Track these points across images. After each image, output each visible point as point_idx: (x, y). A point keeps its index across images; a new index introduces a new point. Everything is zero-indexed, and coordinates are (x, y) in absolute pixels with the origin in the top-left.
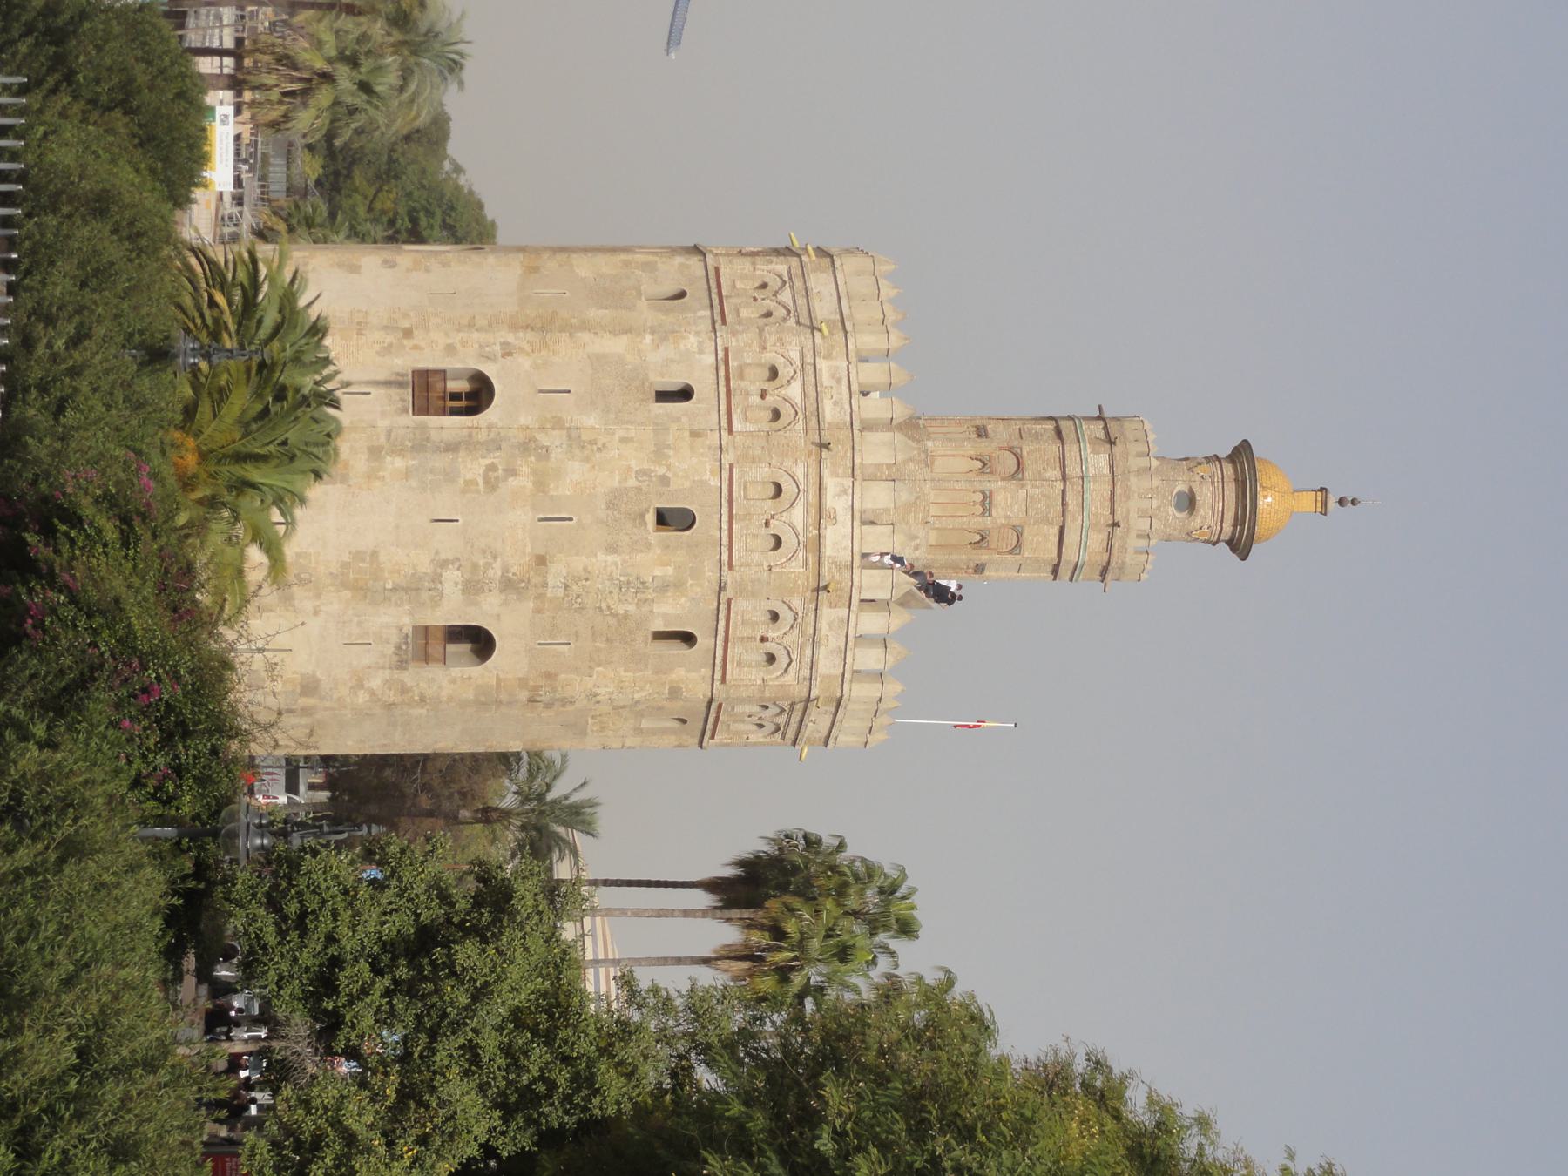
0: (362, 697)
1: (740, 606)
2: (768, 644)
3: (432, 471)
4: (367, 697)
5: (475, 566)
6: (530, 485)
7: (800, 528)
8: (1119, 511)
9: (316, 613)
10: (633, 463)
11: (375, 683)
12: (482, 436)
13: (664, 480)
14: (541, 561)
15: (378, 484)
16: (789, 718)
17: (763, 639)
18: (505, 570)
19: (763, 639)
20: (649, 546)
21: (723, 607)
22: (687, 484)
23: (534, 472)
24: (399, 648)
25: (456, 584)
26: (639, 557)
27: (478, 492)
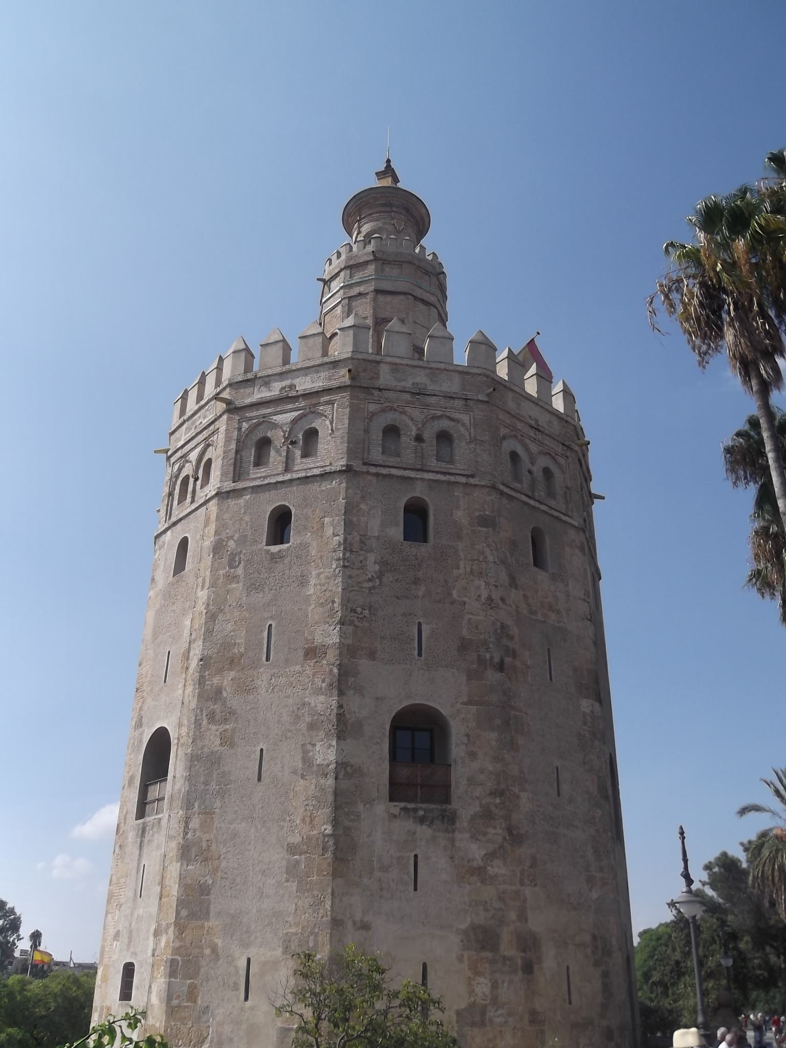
0: (497, 868)
1: (376, 454)
2: (426, 435)
3: (206, 783)
4: (497, 862)
5: (312, 727)
6: (232, 674)
7: (296, 414)
8: (367, 259)
9: (365, 927)
10: (221, 572)
11: (476, 851)
12: (184, 731)
13: (242, 541)
14: (312, 652)
15: (214, 847)
16: (530, 438)
17: (419, 439)
18: (318, 691)
19: (419, 439)
20: (304, 546)
21: (373, 470)
22: (247, 518)
23: (220, 671)
24: (422, 820)
25: (330, 746)
26: (314, 553)
27: (234, 730)
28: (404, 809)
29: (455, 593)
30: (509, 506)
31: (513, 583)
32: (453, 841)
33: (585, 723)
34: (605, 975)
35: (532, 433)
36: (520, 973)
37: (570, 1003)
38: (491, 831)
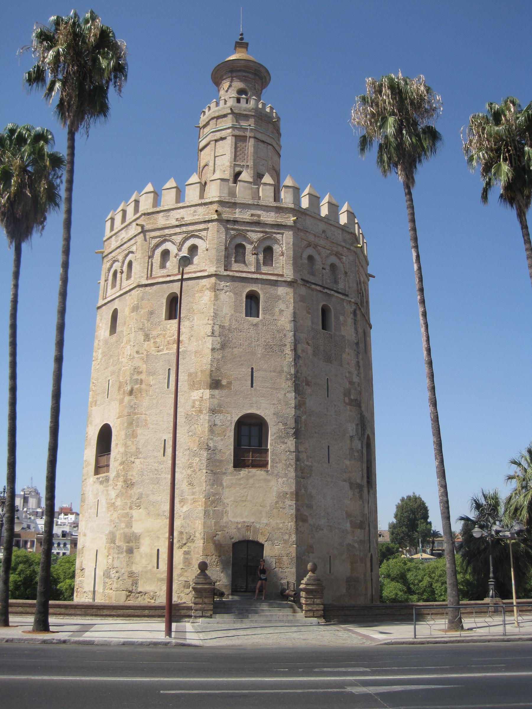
16: (175, 234)
28: (97, 478)
29: (120, 357)
30: (150, 291)
31: (147, 338)
32: (107, 491)
33: (193, 407)
34: (186, 553)
35: (178, 230)
36: (125, 554)
37: (158, 568)
38: (118, 483)
